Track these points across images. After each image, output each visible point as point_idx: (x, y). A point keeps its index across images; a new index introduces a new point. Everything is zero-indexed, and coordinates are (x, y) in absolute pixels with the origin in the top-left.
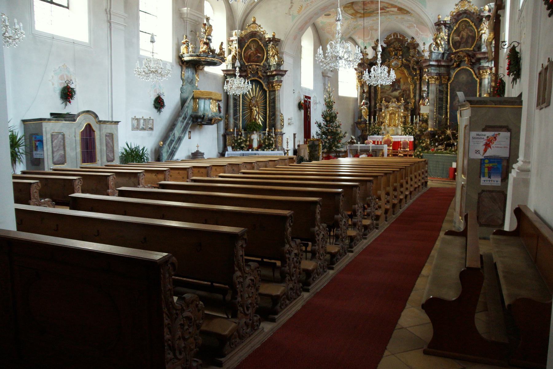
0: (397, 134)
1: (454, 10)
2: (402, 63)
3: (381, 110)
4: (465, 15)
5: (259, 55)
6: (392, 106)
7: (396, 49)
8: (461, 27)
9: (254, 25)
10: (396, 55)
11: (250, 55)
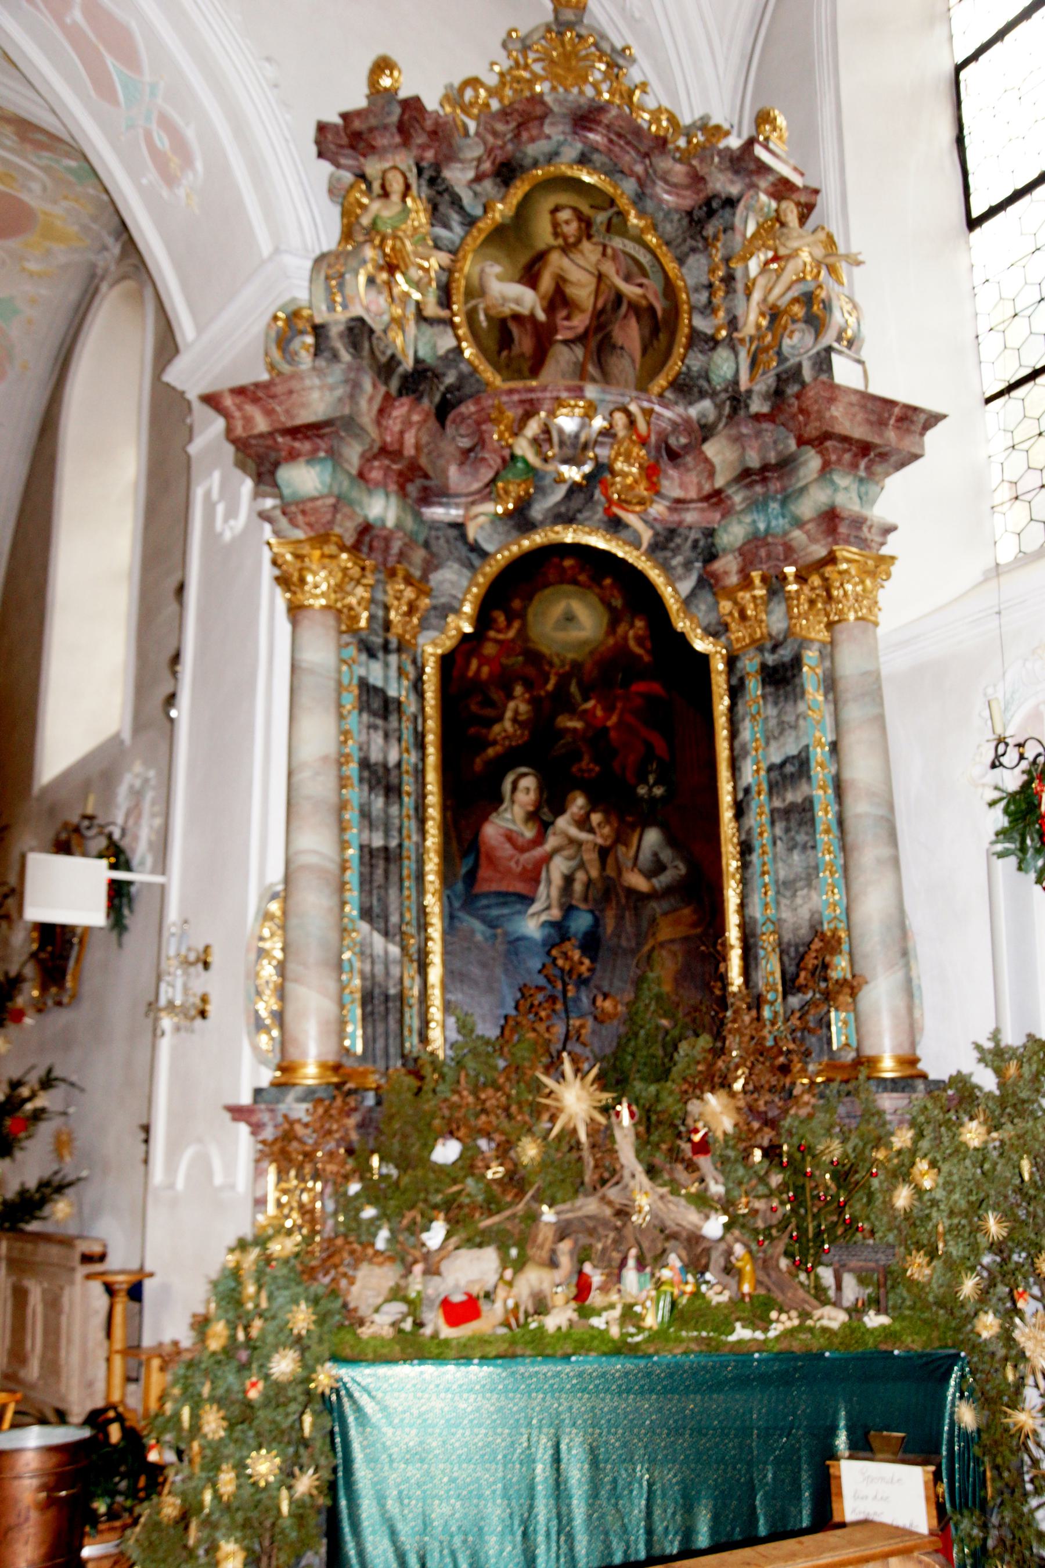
8: (543, 234)
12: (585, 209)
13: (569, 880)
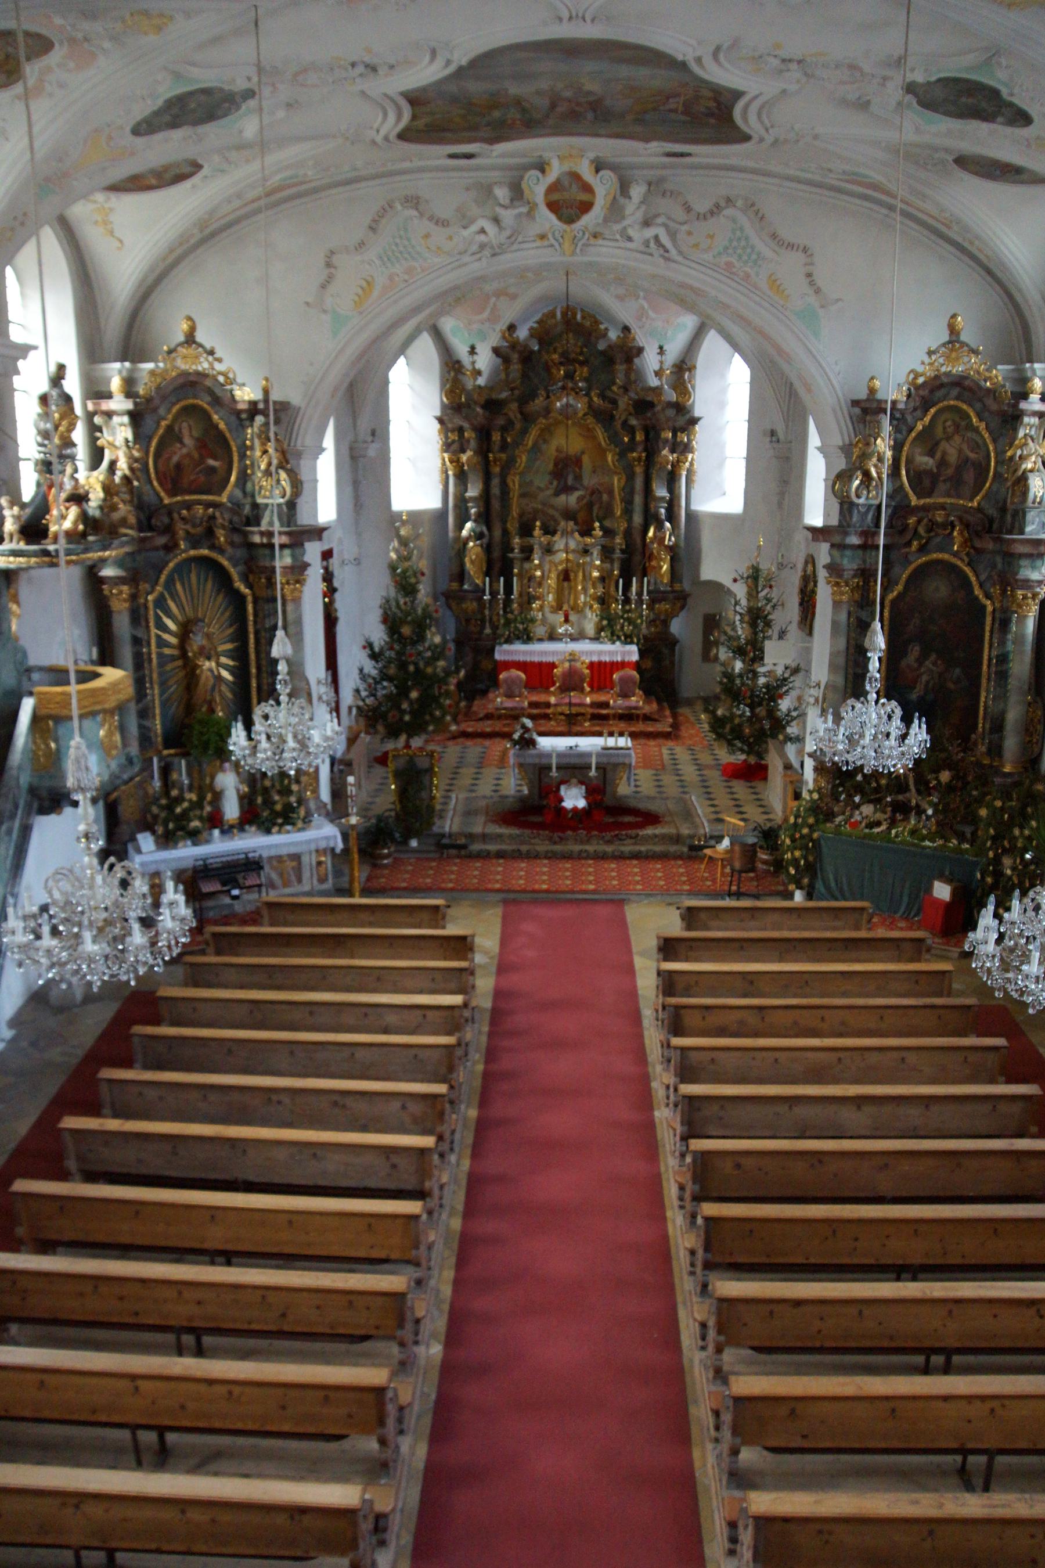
0: (578, 636)
1: (920, 369)
2: (590, 405)
3: (527, 552)
4: (955, 392)
5: (211, 462)
6: (566, 545)
7: (567, 360)
8: (939, 431)
9: (191, 351)
10: (570, 376)
11: (178, 466)
12: (957, 419)
13: (928, 682)
